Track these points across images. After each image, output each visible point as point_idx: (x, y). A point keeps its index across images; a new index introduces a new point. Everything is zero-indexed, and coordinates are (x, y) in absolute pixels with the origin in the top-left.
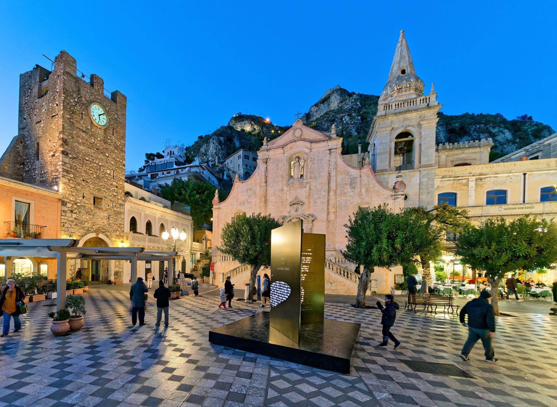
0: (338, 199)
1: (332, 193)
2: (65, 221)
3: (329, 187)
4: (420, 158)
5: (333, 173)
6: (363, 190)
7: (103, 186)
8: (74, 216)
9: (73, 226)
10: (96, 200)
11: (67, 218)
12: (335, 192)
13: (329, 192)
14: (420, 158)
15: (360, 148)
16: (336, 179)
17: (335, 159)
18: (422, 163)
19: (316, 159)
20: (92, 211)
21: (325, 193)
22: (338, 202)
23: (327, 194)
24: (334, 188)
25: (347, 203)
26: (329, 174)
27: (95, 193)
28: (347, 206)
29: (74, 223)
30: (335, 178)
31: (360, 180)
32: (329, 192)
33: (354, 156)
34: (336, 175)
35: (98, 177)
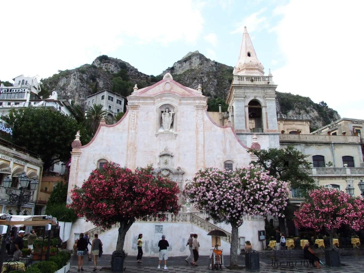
1: (200, 148)
4: (267, 124)
6: (228, 147)
14: (267, 124)
15: (220, 107)
16: (204, 134)
18: (269, 128)
22: (206, 157)
24: (202, 143)
26: (197, 128)
28: (215, 161)
30: (202, 133)
31: (225, 137)
32: (197, 145)
33: (216, 114)
34: (204, 131)
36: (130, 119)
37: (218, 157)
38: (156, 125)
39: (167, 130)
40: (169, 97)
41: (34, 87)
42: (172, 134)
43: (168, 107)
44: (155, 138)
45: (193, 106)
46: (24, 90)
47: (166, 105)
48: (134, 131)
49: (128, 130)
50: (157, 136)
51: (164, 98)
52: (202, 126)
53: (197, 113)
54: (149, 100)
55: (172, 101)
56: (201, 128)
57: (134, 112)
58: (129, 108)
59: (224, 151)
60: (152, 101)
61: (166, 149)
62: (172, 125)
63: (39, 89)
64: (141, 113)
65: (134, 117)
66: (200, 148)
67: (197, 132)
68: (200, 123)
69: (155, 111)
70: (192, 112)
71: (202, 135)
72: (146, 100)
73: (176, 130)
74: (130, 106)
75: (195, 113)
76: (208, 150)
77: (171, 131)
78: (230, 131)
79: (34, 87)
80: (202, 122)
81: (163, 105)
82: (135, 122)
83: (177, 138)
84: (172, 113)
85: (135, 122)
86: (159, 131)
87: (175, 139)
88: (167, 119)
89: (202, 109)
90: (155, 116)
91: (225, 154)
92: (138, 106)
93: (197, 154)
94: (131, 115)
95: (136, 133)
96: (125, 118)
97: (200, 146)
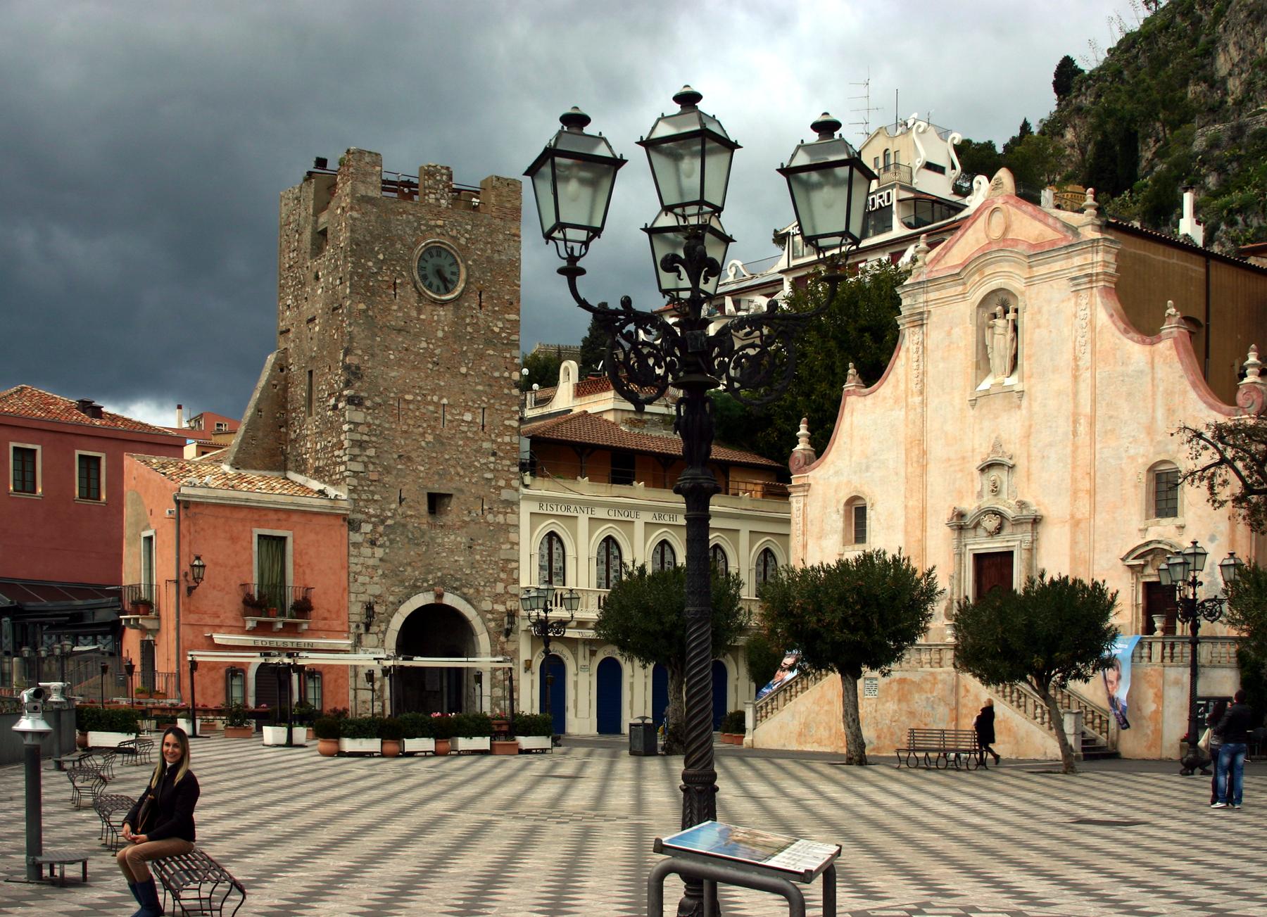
0: (1098, 446)
1: (1083, 429)
2: (359, 568)
3: (1076, 405)
5: (1086, 360)
6: (1160, 413)
7: (452, 462)
8: (379, 552)
9: (376, 579)
10: (436, 502)
11: (361, 560)
12: (1092, 423)
13: (1075, 422)
17: (1088, 311)
19: (1045, 309)
20: (423, 534)
21: (1064, 426)
23: (1071, 428)
24: (1088, 410)
25: (1120, 458)
26: (1076, 359)
27: (430, 485)
28: (1122, 469)
29: (380, 572)
30: (1087, 374)
31: (1153, 379)
32: (1075, 422)
34: (1093, 367)
35: (438, 438)
36: (908, 359)
37: (1132, 452)
38: (969, 370)
39: (1000, 379)
40: (1000, 261)
41: (930, 166)
42: (1010, 391)
43: (1005, 297)
44: (972, 412)
45: (1064, 281)
46: (889, 194)
47: (999, 293)
48: (920, 398)
49: (907, 396)
50: (973, 406)
51: (988, 271)
52: (1089, 347)
53: (1076, 304)
54: (951, 287)
55: (1009, 275)
56: (1086, 360)
57: (916, 336)
58: (903, 325)
59: (1150, 430)
60: (960, 288)
61: (997, 446)
62: (1015, 357)
63: (953, 167)
64: (935, 334)
65: (917, 352)
66: (1083, 429)
67: (1076, 378)
68: (1083, 340)
69: (968, 320)
70: (1063, 301)
71: (1089, 381)
72: (944, 288)
73: (1021, 379)
74: (905, 317)
75: (1070, 307)
76: (1106, 432)
77: (1013, 381)
78: (1168, 353)
79: (930, 166)
80: (1088, 335)
81: (989, 294)
82: (921, 367)
83: (1025, 403)
84: (1011, 316)
85: (921, 367)
86: (978, 389)
87: (1019, 407)
88: (1000, 341)
89: (1088, 286)
90: (965, 336)
91: (1152, 440)
92: (922, 313)
93: (1075, 448)
94: (911, 346)
95: (924, 404)
96: (897, 361)
97: (1082, 421)
